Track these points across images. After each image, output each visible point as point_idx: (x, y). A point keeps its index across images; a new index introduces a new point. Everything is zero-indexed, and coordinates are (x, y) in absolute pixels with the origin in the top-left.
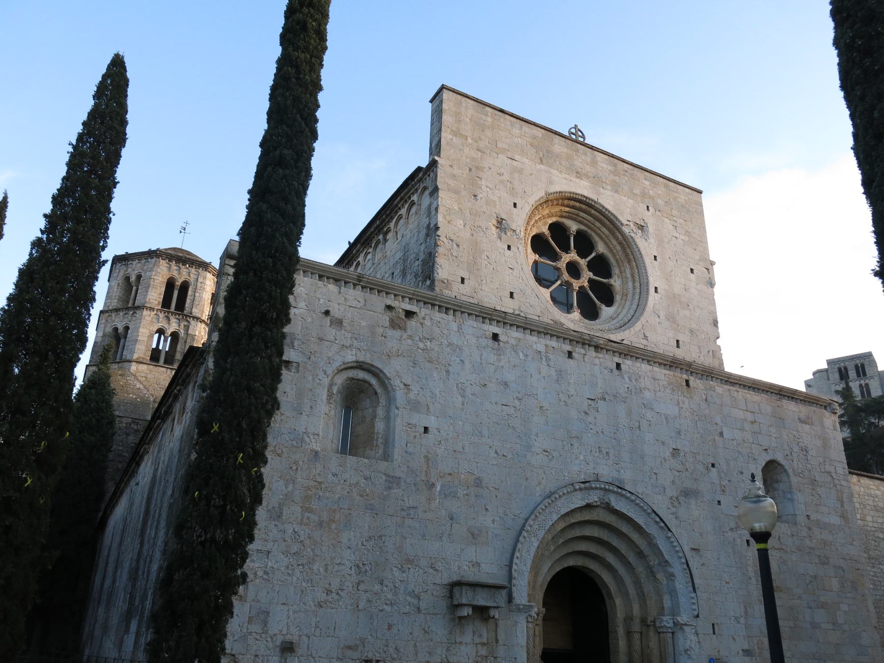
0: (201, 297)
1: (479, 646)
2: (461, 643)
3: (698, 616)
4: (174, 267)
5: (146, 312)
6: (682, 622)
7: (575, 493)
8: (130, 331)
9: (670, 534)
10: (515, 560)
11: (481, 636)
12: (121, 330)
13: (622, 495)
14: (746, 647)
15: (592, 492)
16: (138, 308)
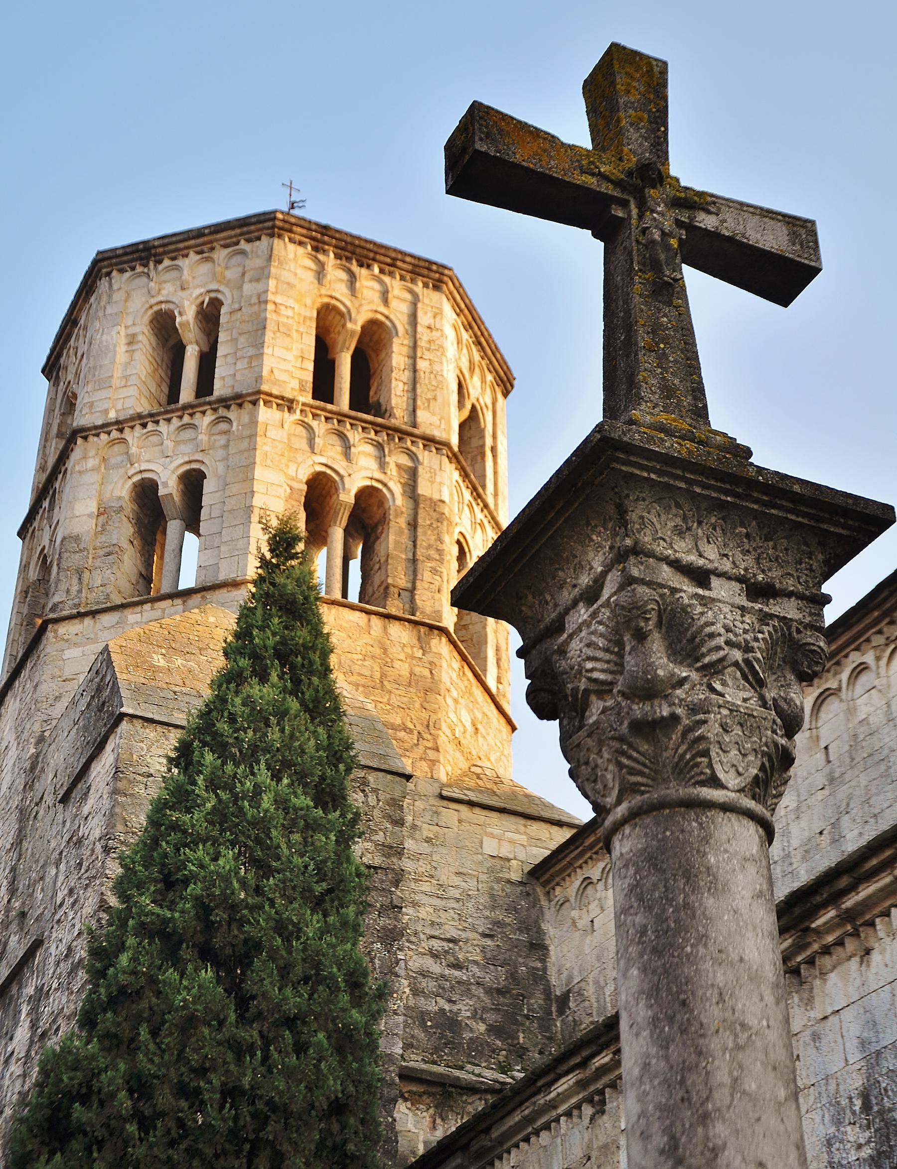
0: (437, 375)
4: (335, 274)
5: (266, 414)
8: (209, 486)
12: (169, 486)
16: (237, 400)
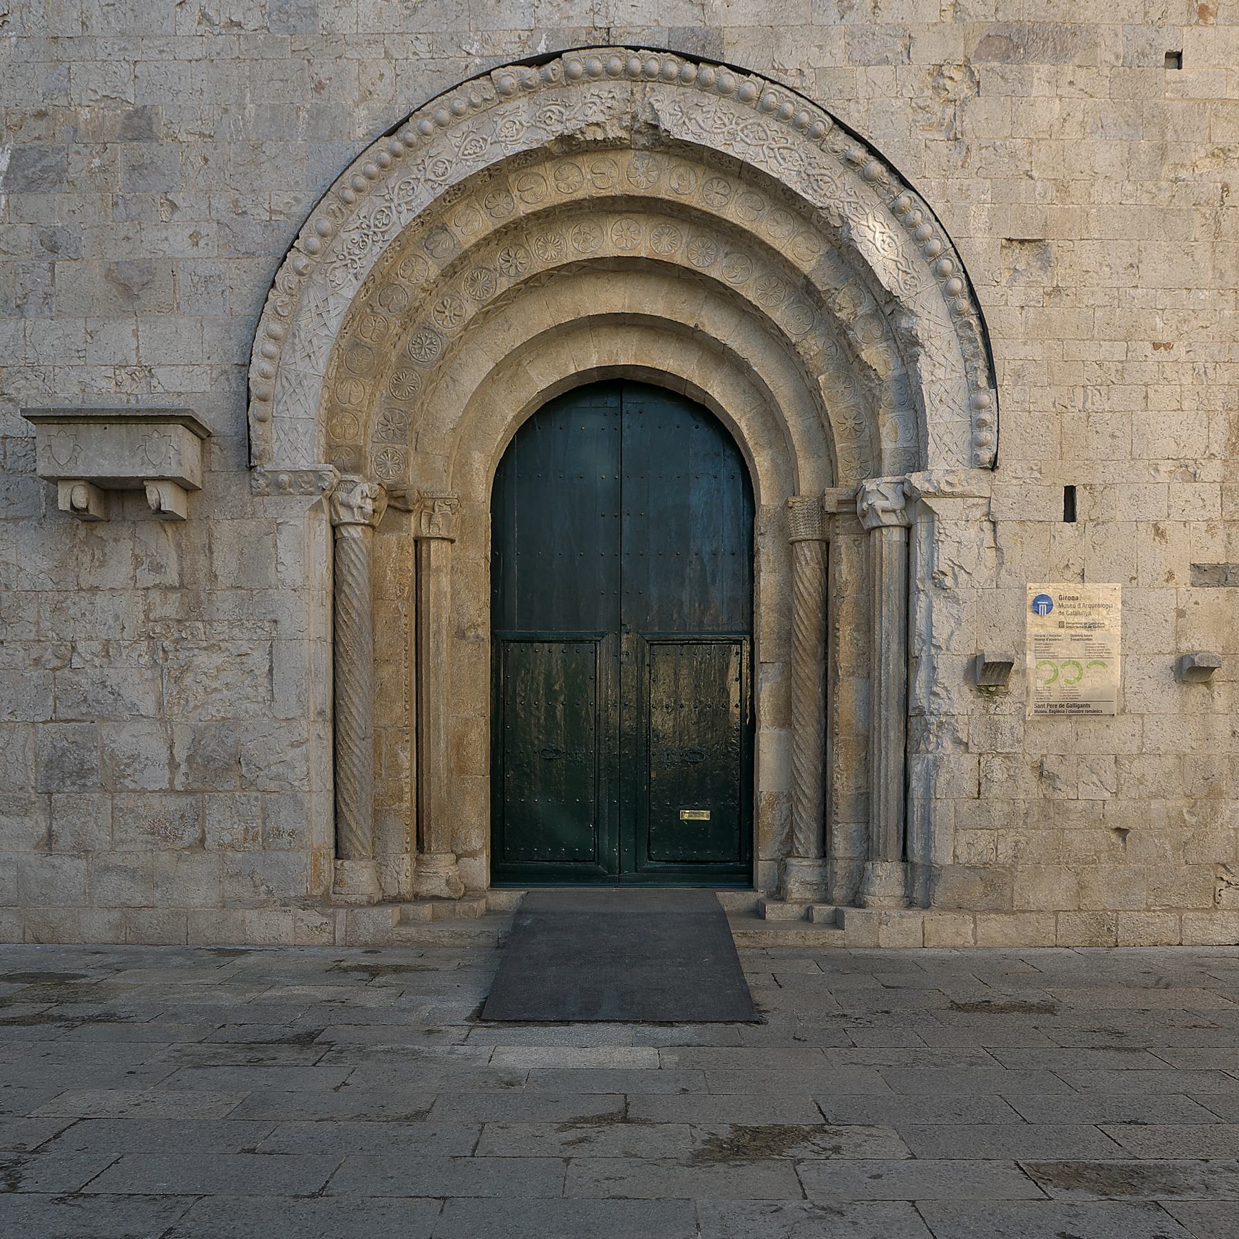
1: (155, 596)
2: (94, 589)
3: (994, 466)
6: (927, 486)
7: (509, 106)
9: (905, 198)
10: (263, 345)
11: (157, 568)
13: (704, 86)
14: (1214, 554)
15: (576, 94)
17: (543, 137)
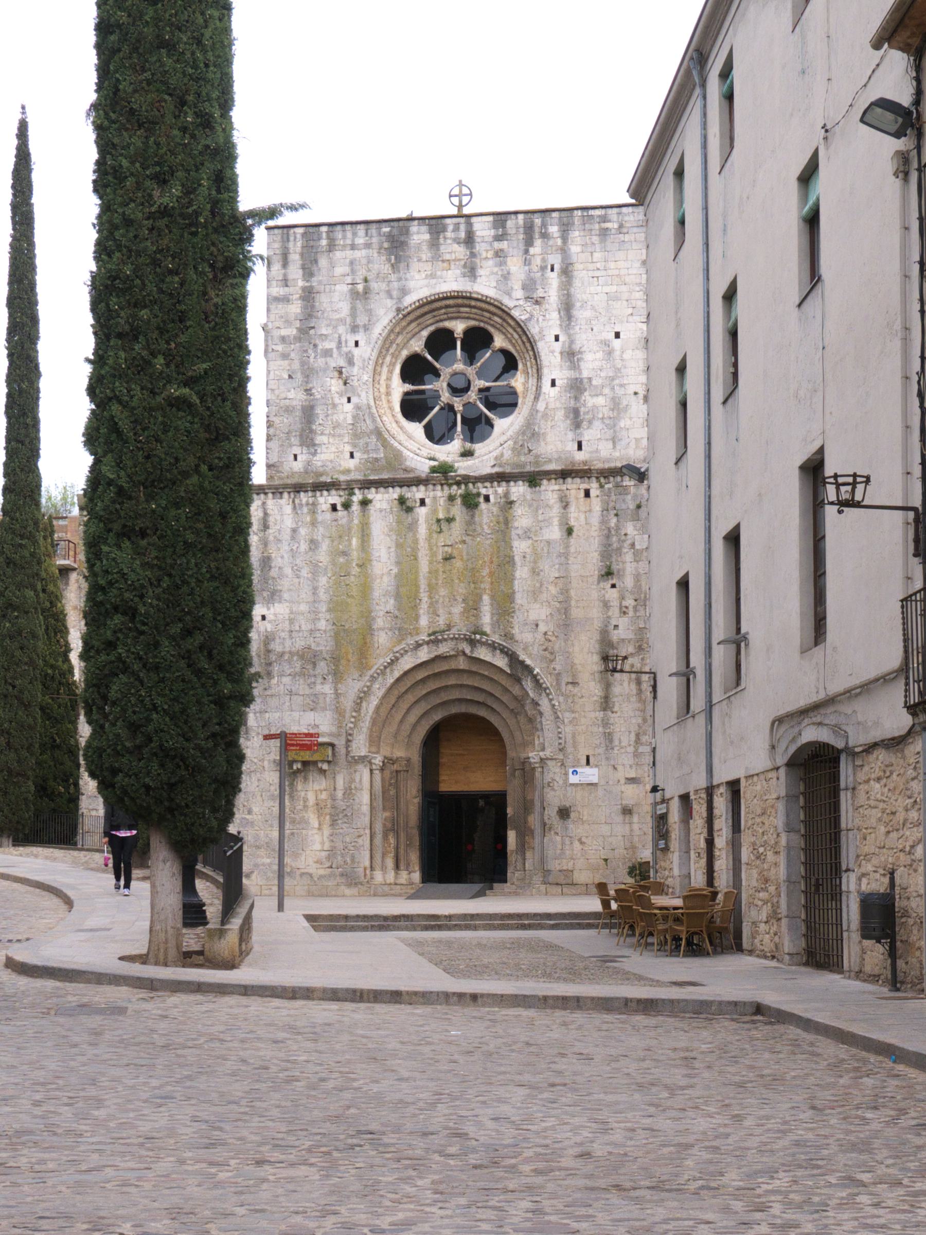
14: (632, 774)
17: (432, 656)
